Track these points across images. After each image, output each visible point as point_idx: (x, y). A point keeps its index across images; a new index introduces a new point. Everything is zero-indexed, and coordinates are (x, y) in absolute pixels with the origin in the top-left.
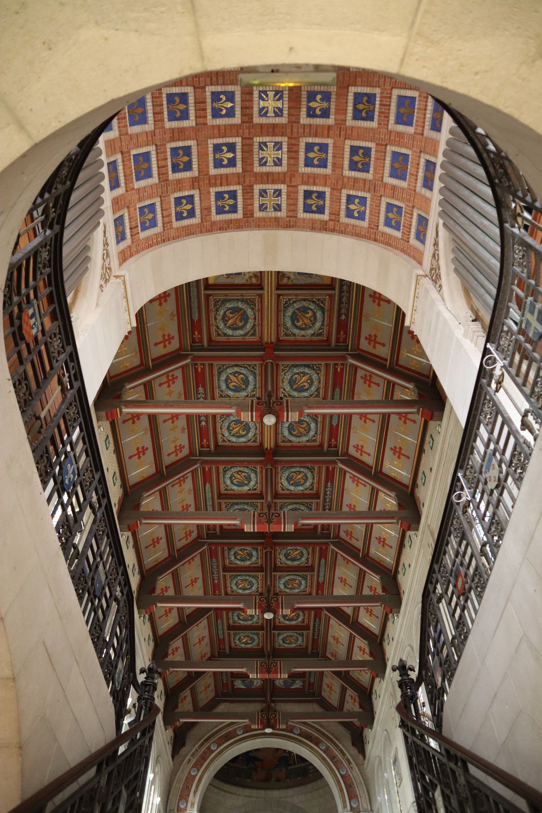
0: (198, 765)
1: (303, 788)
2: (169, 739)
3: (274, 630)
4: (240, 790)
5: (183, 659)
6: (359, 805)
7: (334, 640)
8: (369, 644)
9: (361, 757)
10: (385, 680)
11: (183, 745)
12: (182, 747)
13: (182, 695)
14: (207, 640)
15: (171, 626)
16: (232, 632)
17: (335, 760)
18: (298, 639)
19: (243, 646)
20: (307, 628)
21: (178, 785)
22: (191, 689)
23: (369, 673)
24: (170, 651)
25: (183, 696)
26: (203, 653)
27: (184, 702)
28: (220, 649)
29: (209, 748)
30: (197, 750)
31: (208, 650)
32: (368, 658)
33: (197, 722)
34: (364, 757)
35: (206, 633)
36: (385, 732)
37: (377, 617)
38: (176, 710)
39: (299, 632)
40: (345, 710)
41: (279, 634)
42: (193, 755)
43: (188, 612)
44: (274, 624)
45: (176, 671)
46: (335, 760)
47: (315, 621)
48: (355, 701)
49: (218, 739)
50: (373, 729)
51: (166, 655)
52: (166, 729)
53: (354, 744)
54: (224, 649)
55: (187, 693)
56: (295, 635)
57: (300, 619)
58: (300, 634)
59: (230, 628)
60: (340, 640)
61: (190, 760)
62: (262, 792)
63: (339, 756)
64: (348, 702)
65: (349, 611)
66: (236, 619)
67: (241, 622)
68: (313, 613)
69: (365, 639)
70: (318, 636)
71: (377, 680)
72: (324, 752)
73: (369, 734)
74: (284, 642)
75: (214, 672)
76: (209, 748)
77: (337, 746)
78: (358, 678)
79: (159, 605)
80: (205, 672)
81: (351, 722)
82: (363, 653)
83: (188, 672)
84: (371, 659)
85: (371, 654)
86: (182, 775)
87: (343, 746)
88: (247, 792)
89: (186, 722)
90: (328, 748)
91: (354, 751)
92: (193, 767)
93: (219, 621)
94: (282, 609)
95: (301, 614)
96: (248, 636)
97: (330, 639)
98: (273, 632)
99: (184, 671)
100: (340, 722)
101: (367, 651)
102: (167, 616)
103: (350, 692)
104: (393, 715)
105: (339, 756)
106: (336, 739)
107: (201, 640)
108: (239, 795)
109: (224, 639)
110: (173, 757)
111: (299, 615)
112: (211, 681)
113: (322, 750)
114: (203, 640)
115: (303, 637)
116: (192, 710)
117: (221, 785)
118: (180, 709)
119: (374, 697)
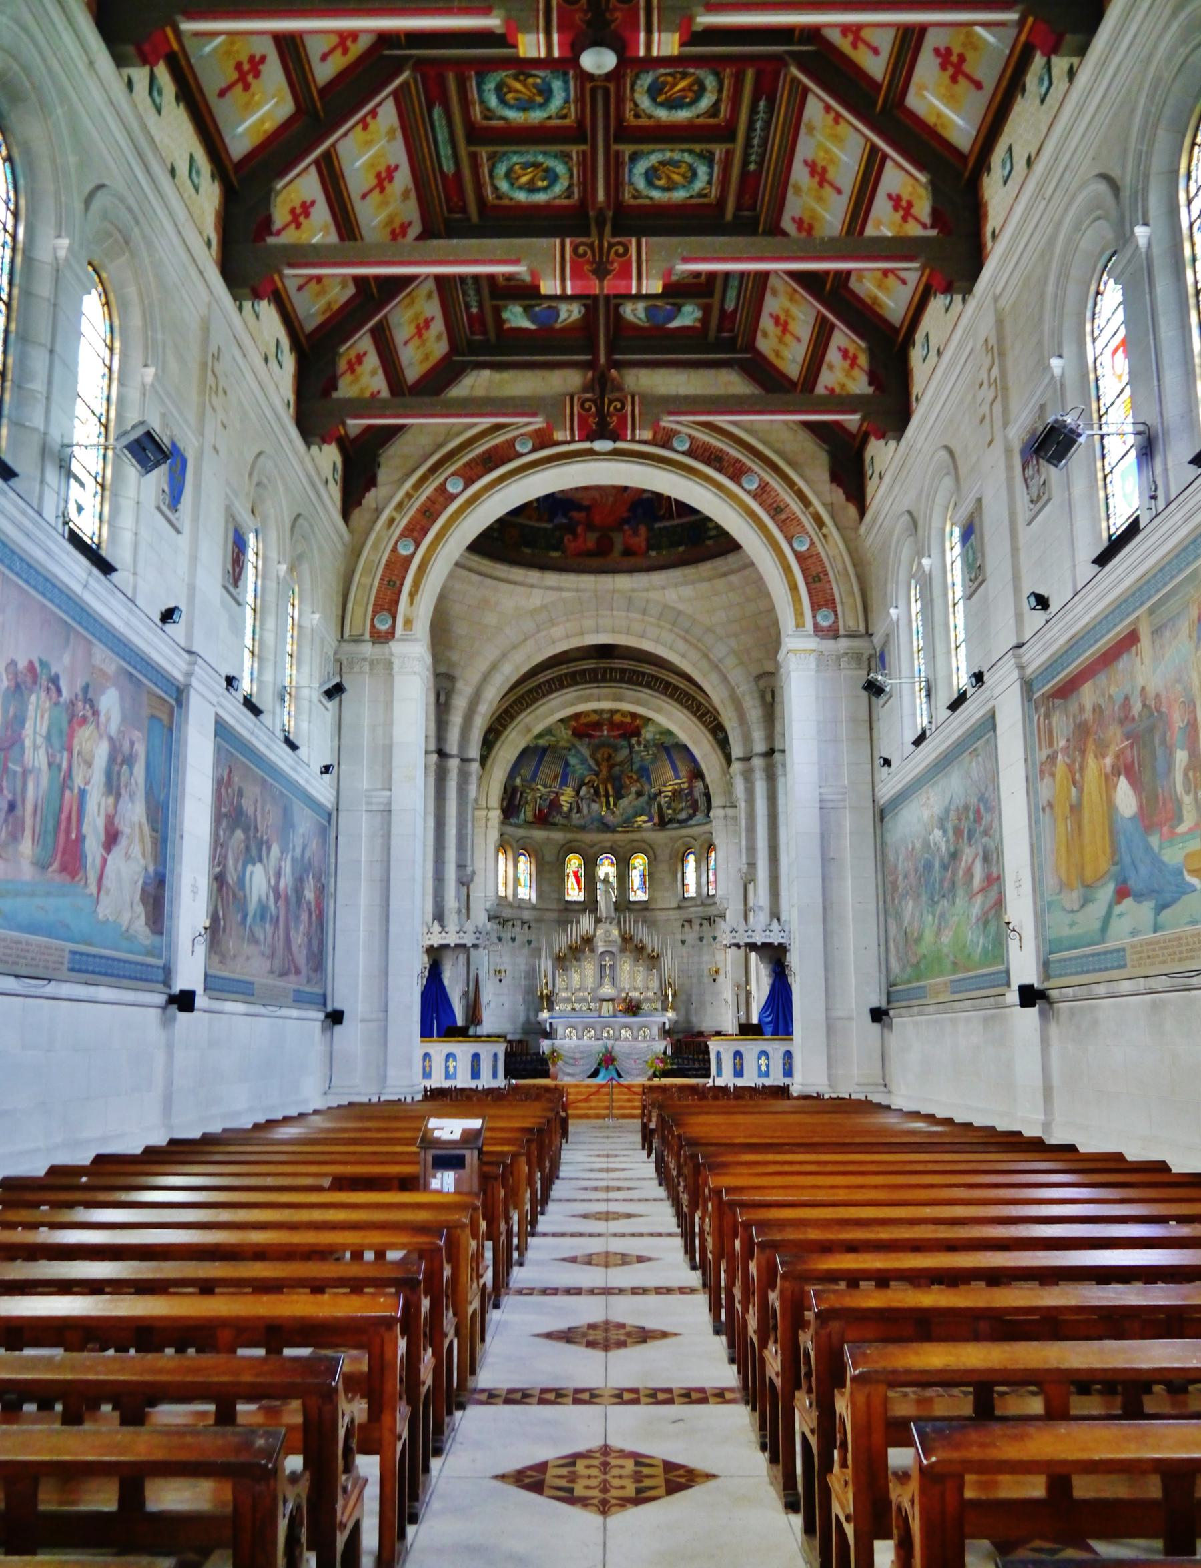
0: (416, 531)
1: (689, 571)
2: (327, 471)
3: (619, 139)
4: (534, 576)
5: (333, 238)
6: (836, 622)
7: (813, 173)
8: (935, 187)
9: (852, 510)
10: (972, 303)
11: (372, 482)
12: (368, 489)
13: (348, 351)
14: (403, 178)
15: (269, 126)
16: (484, 152)
17: (783, 516)
18: (694, 174)
19: (522, 197)
20: (726, 133)
21: (367, 583)
22: (373, 331)
23: (913, 278)
24: (280, 216)
25: (352, 354)
26: (397, 225)
27: (359, 370)
28: (451, 211)
29: (442, 489)
30: (409, 495)
31: (411, 211)
32: (913, 230)
33: (401, 427)
34: (862, 510)
35: (397, 154)
36: (943, 454)
37: (978, 85)
38: (335, 395)
39: (697, 148)
40: (820, 389)
41: (634, 158)
42: (400, 505)
43: (324, 72)
44: (620, 118)
45: (319, 279)
46: (783, 516)
47: (753, 110)
48: (854, 363)
49: (465, 465)
50: (903, 441)
51: (265, 226)
52: (308, 444)
53: (835, 478)
54: (464, 210)
55: (363, 342)
56: (687, 157)
57: (705, 103)
58: (701, 156)
59: (477, 135)
60: (831, 174)
61: (391, 521)
62: (587, 581)
63: (795, 506)
64: (831, 367)
65: (876, 66)
66: (493, 101)
67: (511, 114)
68: (750, 74)
69: (921, 167)
70: (760, 164)
71: (937, 304)
72: (755, 496)
73: (880, 452)
74: (650, 184)
75: (439, 280)
76: (442, 489)
77: (791, 483)
78: (875, 299)
79: (187, 26)
80: (411, 279)
81: (837, 423)
82: (905, 219)
83: (357, 280)
84: (933, 233)
85: (938, 217)
86: (375, 555)
87: (807, 481)
88: (552, 578)
89: (370, 427)
90: (764, 487)
91: (838, 495)
92: (402, 535)
93: (437, 112)
94: (649, 31)
95: (710, 82)
96: (537, 165)
97: (799, 173)
98: (614, 147)
99: (344, 276)
100: (806, 424)
101: (923, 209)
102: (247, 87)
103: (842, 338)
104: (985, 408)
105: (795, 506)
106: (790, 463)
107: (384, 178)
108: (532, 586)
109: (458, 173)
110: (346, 514)
111: (702, 89)
112: (432, 308)
113: (748, 492)
114: (390, 178)
115: (710, 165)
116: (385, 393)
117: (486, 565)
118: (346, 389)
119: (916, 354)
